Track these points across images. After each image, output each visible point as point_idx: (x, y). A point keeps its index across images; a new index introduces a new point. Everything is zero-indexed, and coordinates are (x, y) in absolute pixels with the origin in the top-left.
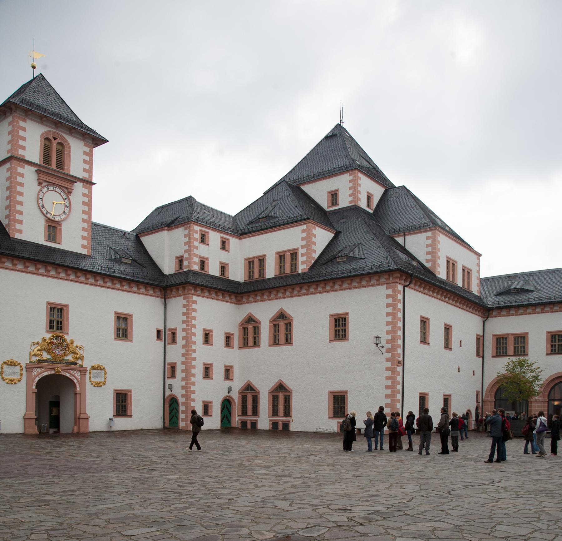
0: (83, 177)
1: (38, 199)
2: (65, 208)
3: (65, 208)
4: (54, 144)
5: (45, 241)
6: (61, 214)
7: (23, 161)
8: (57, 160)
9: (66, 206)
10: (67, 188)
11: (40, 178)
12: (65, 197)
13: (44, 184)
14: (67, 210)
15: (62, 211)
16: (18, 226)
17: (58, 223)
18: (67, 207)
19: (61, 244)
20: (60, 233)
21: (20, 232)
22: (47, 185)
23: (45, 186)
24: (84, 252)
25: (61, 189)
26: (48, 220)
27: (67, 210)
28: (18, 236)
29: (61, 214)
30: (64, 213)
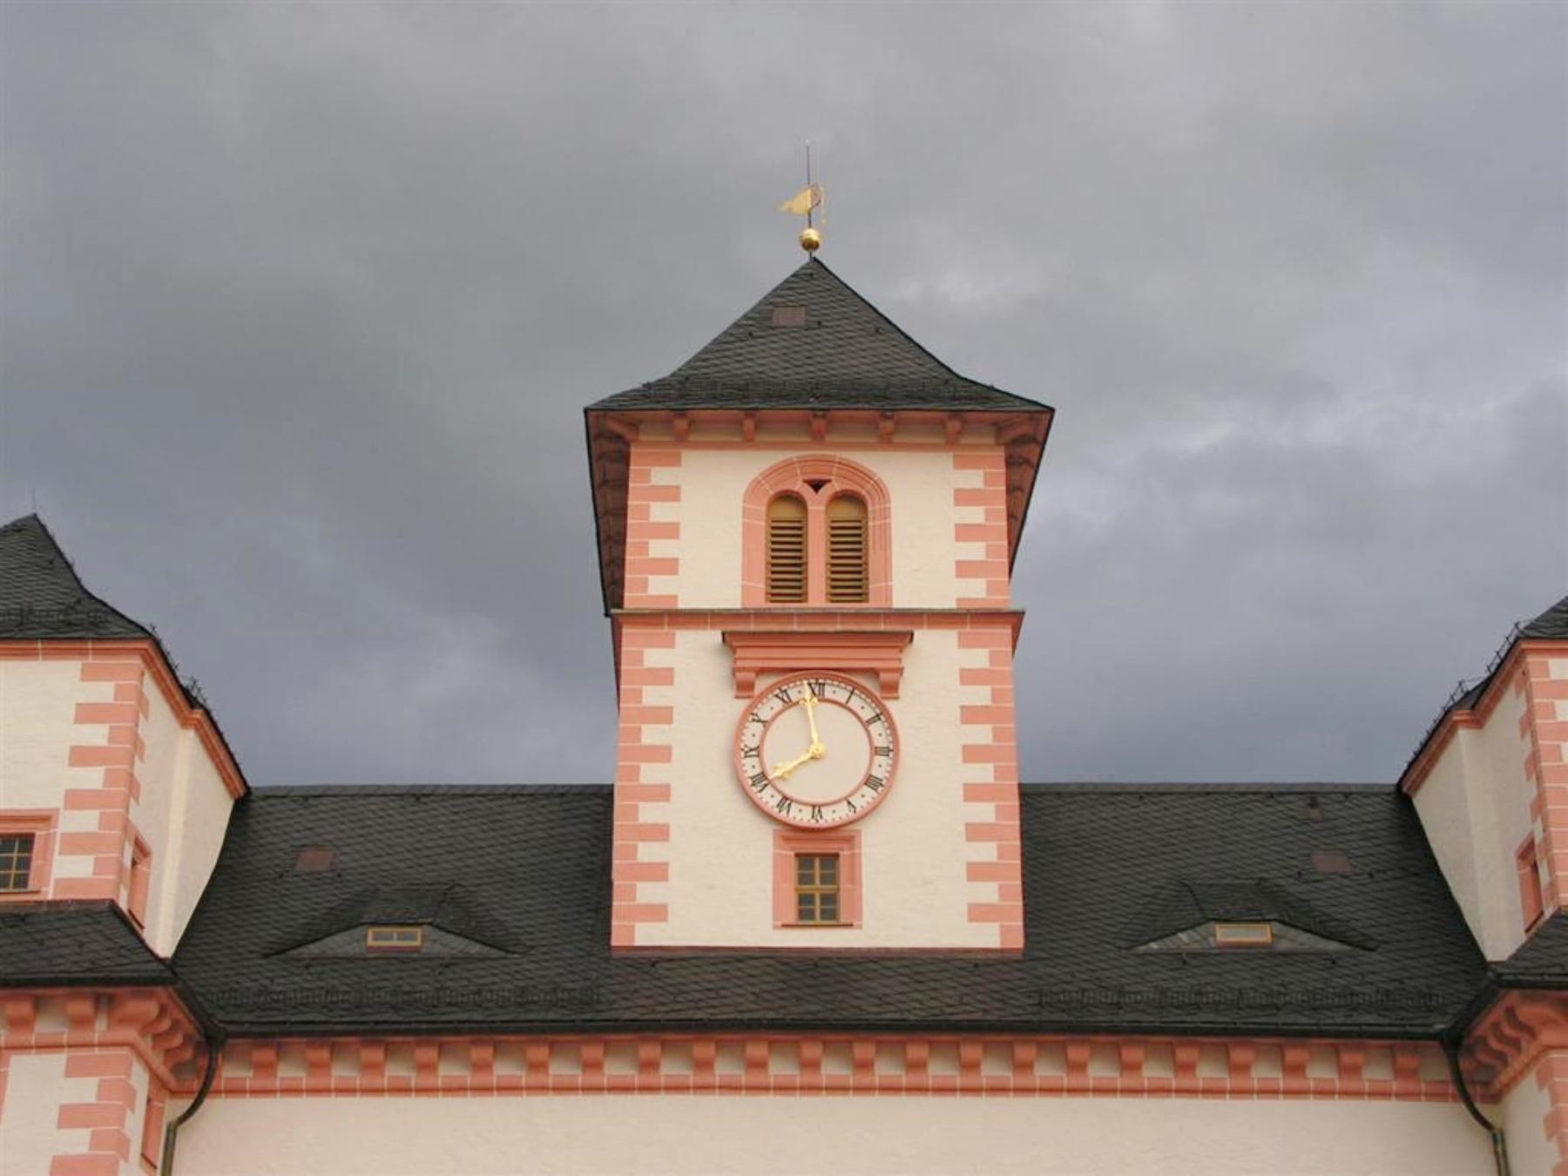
0: (959, 600)
1: (739, 751)
2: (871, 761)
3: (871, 761)
4: (817, 504)
5: (775, 927)
6: (852, 794)
7: (666, 620)
8: (834, 568)
9: (876, 751)
10: (873, 673)
11: (740, 664)
12: (867, 714)
13: (762, 684)
14: (881, 768)
15: (860, 777)
16: (647, 892)
17: (843, 834)
18: (885, 752)
19: (860, 927)
20: (855, 879)
21: (658, 913)
22: (777, 685)
23: (770, 690)
24: (988, 937)
25: (848, 682)
26: (792, 832)
27: (881, 768)
28: (646, 935)
29: (852, 794)
30: (871, 781)
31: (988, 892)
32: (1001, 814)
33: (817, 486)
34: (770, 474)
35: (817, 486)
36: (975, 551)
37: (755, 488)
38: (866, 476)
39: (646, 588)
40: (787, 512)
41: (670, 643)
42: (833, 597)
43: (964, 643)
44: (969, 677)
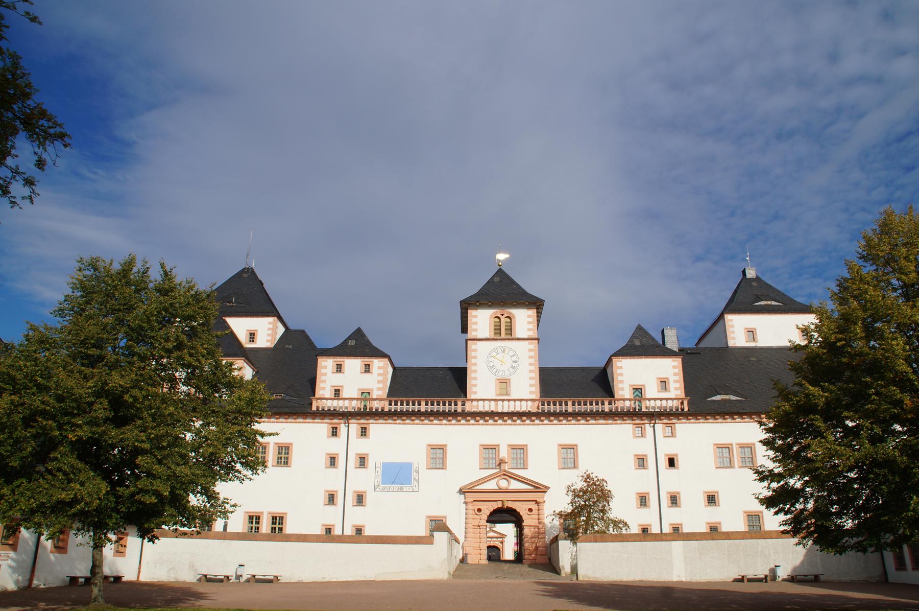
0: (528, 336)
4: (502, 318)
21: (475, 393)
31: (533, 389)
32: (536, 375)
33: (502, 315)
34: (493, 313)
35: (502, 315)
36: (531, 326)
37: (491, 316)
38: (511, 313)
39: (471, 334)
40: (497, 320)
41: (476, 344)
42: (506, 335)
43: (529, 344)
44: (530, 350)
